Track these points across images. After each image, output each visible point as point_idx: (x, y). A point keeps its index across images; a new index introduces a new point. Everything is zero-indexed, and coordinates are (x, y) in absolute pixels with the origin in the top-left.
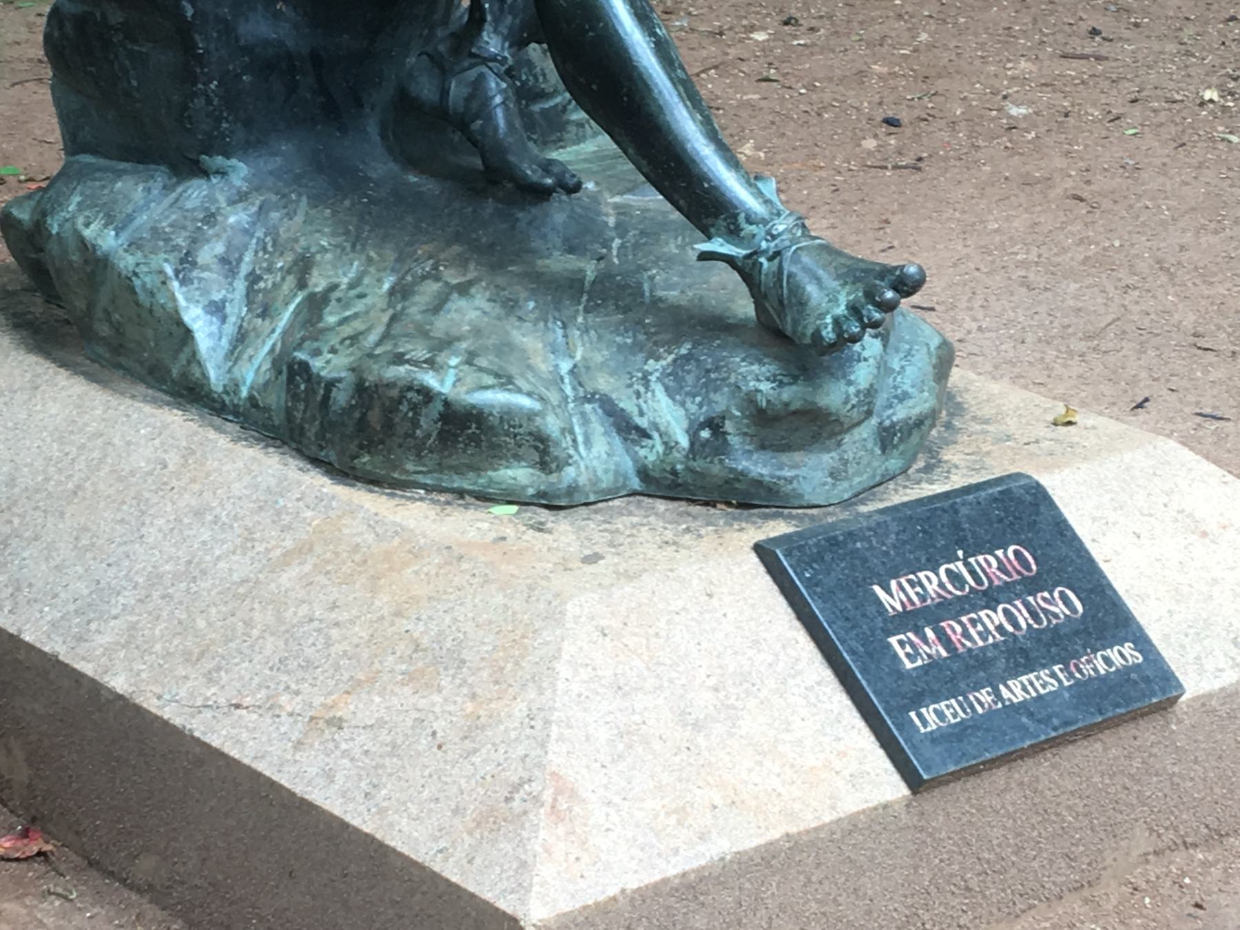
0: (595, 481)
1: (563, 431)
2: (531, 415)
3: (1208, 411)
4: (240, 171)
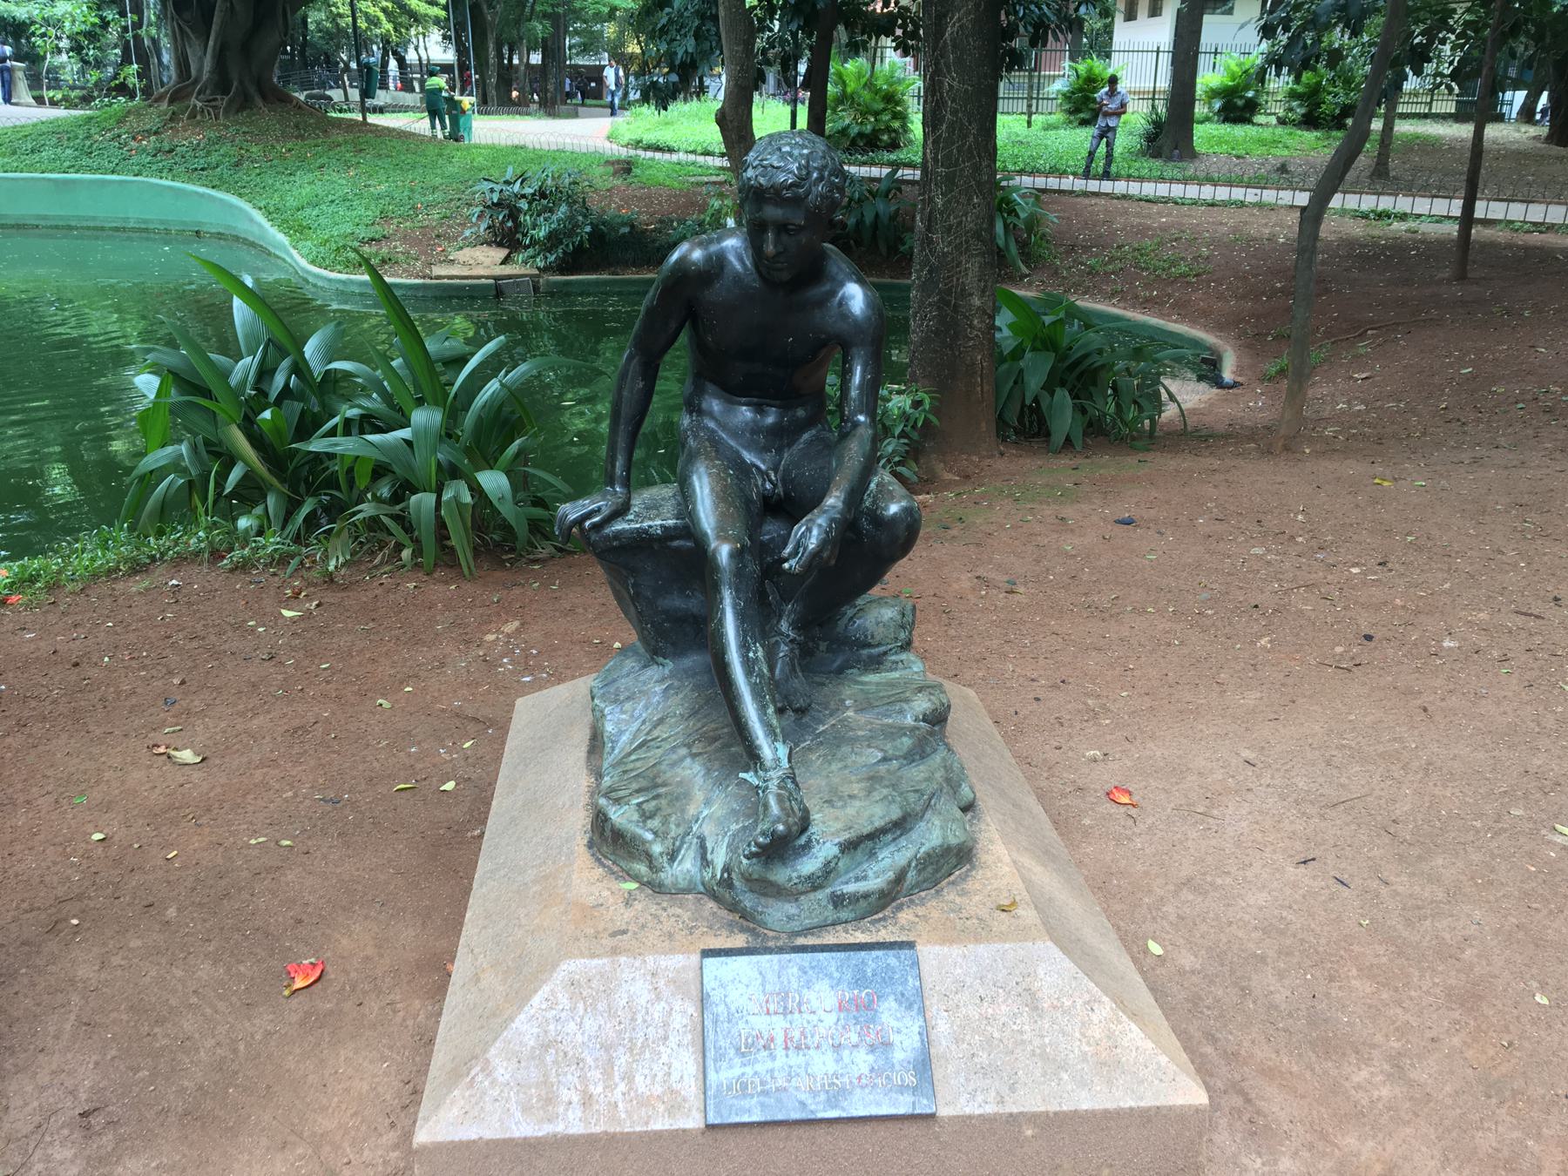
0: (675, 884)
1: (661, 854)
2: (644, 842)
3: (1345, 877)
4: (670, 665)
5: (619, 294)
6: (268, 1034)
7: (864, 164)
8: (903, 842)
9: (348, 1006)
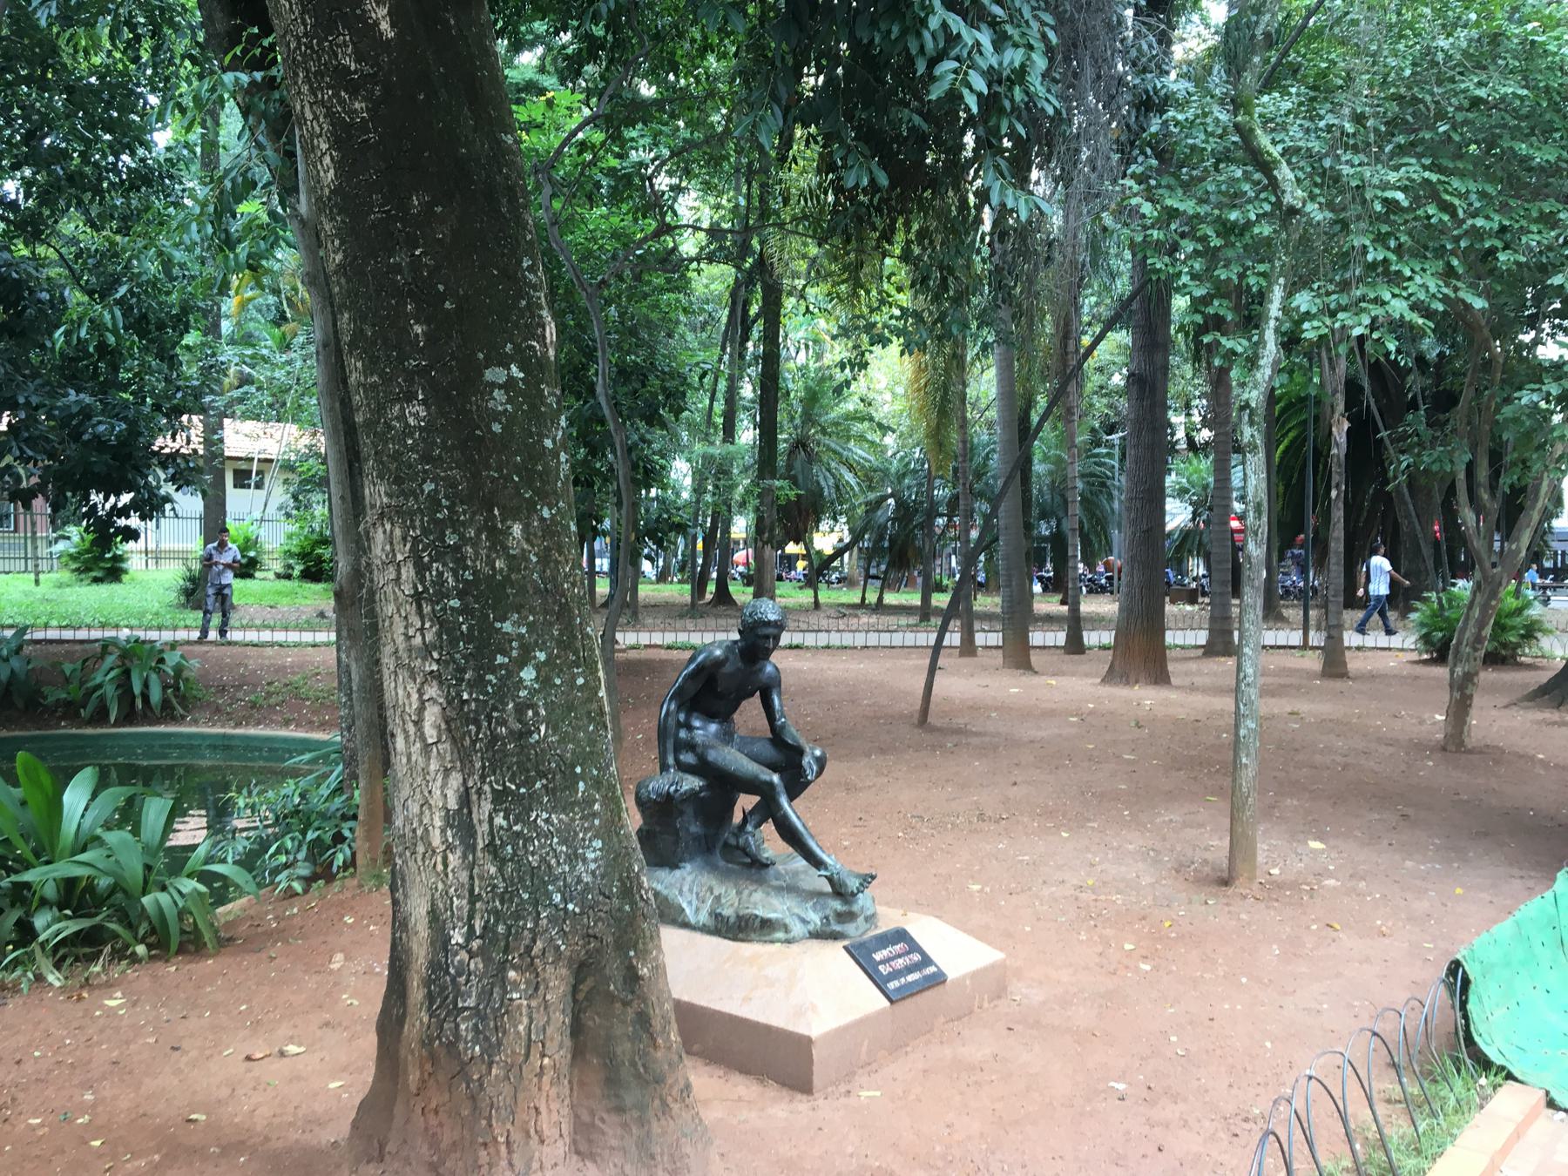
4: (688, 867)
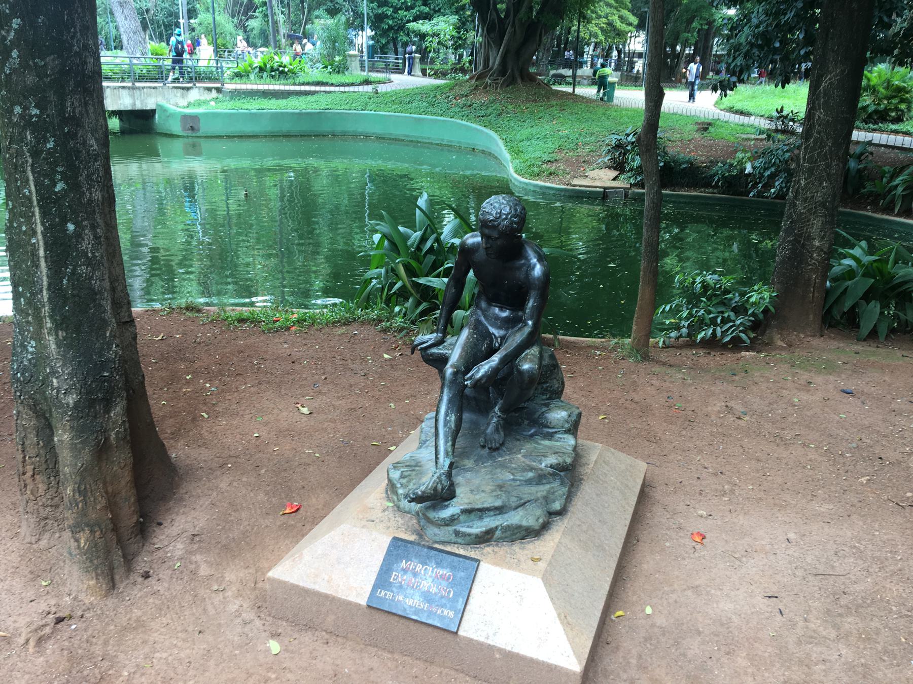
5: (674, 202)
6: (267, 526)
7: (874, 130)
8: (499, 517)
9: (299, 525)
